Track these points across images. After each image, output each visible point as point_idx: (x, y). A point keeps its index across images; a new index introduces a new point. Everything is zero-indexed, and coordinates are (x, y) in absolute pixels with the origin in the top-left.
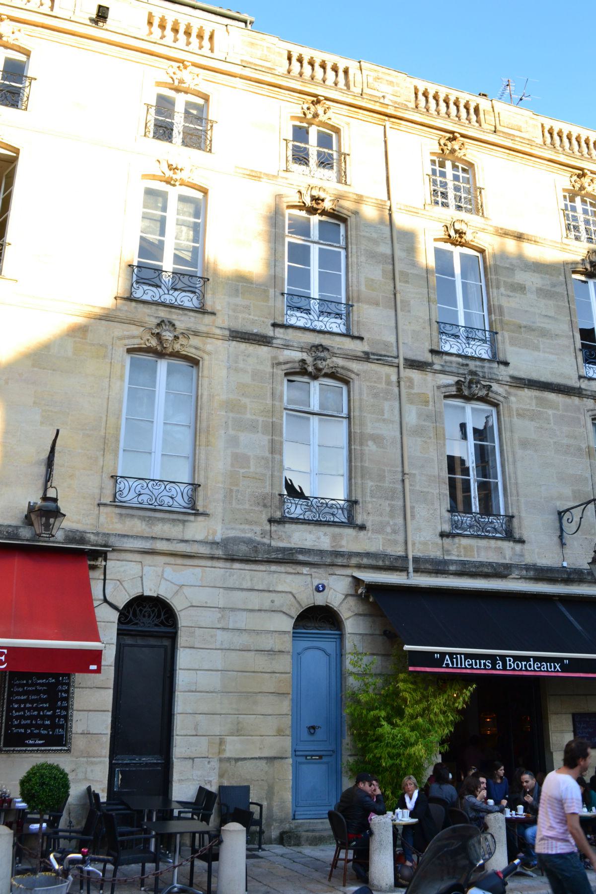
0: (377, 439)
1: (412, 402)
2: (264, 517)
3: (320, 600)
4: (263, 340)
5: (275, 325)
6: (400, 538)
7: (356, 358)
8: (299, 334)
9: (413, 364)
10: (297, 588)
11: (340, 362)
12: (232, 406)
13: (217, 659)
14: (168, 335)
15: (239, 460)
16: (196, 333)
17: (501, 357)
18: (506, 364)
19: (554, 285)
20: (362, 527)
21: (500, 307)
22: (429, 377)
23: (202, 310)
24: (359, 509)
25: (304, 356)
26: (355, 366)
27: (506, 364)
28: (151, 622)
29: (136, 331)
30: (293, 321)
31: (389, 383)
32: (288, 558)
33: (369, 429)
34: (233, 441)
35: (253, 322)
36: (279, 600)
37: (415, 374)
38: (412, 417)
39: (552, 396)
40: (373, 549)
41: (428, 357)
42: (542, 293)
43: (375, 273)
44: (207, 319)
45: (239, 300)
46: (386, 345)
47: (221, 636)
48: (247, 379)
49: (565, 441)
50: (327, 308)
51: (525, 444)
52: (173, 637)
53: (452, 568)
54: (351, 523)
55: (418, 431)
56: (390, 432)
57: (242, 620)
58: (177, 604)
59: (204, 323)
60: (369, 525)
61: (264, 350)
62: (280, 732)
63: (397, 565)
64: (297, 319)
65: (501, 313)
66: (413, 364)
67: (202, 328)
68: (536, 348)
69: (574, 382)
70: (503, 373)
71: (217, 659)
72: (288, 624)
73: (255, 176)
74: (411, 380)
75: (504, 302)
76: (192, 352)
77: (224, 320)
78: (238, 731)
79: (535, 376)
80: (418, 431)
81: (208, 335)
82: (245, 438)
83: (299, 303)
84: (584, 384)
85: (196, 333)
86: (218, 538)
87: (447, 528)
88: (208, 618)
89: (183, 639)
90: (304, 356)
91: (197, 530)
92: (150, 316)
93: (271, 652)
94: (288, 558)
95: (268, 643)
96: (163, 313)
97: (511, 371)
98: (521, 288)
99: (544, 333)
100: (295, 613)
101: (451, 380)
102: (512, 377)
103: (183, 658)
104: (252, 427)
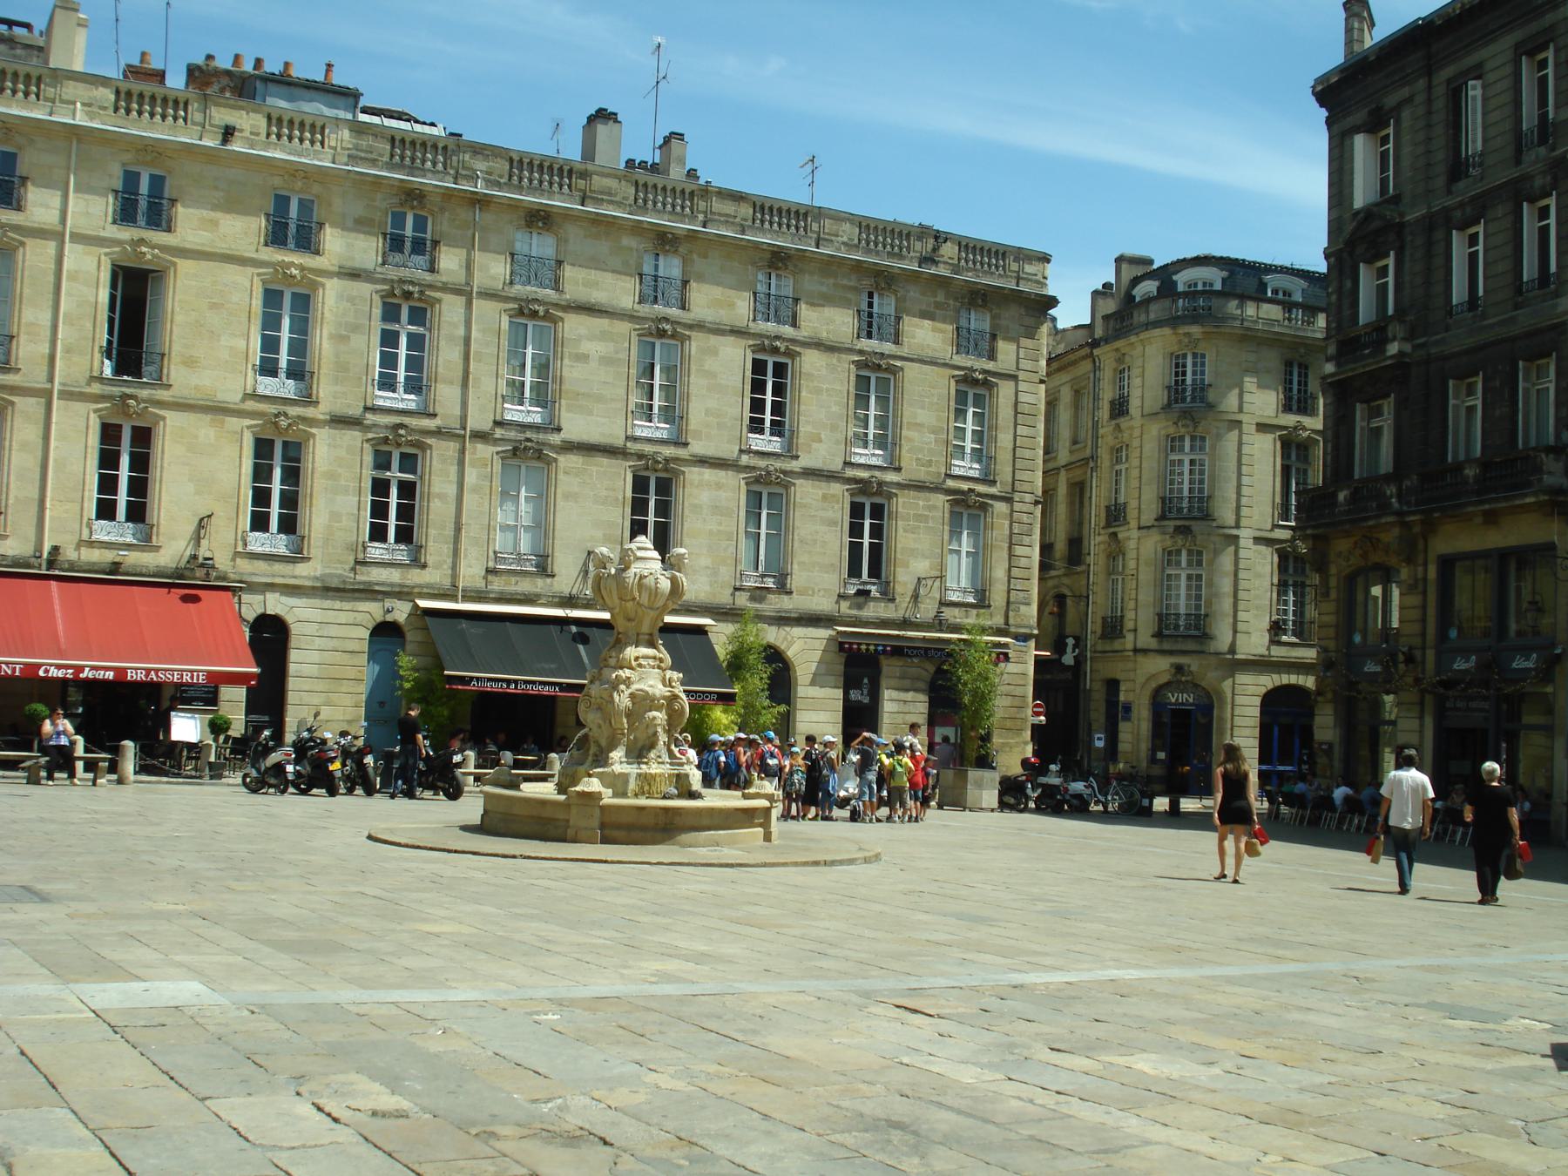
3: (389, 618)
5: (366, 409)
10: (373, 611)
12: (331, 476)
13: (316, 656)
15: (335, 516)
30: (380, 403)
35: (349, 406)
36: (360, 617)
42: (606, 361)
45: (338, 388)
47: (318, 642)
48: (342, 453)
49: (605, 493)
51: (567, 497)
55: (475, 490)
58: (289, 619)
59: (309, 412)
60: (430, 563)
68: (590, 413)
69: (619, 441)
70: (555, 439)
71: (316, 656)
72: (366, 634)
73: (354, 275)
80: (475, 490)
86: (318, 574)
88: (311, 629)
89: (293, 642)
91: (302, 569)
97: (563, 435)
98: (583, 358)
99: (600, 399)
100: (371, 625)
103: (294, 655)
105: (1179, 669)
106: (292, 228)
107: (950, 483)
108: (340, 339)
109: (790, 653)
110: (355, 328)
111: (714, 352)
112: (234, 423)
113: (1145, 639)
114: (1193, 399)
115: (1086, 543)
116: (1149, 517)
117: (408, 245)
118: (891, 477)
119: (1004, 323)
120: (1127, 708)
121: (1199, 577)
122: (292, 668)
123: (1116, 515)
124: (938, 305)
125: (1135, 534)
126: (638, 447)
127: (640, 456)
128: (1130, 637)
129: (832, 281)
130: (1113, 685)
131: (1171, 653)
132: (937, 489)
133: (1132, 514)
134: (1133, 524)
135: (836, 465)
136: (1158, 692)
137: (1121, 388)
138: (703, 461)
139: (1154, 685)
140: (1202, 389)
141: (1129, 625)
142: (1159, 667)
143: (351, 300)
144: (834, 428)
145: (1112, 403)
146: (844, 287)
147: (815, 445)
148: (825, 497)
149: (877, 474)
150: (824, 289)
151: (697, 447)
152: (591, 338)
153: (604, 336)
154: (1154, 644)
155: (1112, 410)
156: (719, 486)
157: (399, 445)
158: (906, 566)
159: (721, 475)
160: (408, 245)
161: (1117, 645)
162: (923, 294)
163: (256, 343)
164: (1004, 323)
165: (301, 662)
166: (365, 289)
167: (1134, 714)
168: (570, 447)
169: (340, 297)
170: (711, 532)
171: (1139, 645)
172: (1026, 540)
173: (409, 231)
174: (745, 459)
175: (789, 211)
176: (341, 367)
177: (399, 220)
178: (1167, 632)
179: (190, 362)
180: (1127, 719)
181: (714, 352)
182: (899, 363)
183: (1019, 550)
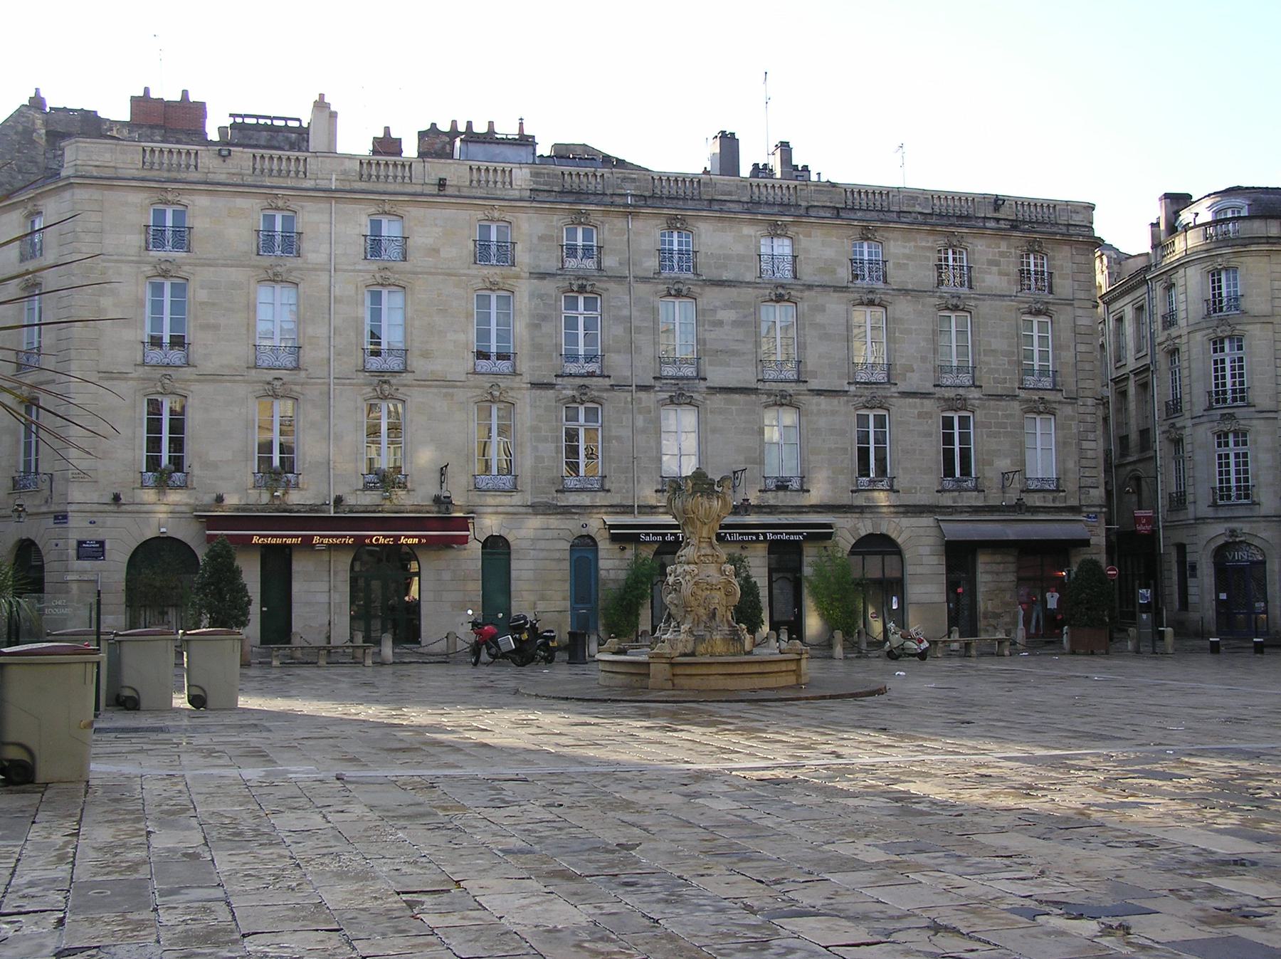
0: (618, 438)
1: (640, 413)
2: (553, 490)
4: (550, 386)
6: (631, 495)
7: (607, 390)
8: (571, 379)
9: (642, 388)
10: (572, 526)
11: (596, 394)
12: (534, 429)
13: (531, 565)
14: (496, 393)
15: (538, 459)
16: (512, 389)
17: (702, 375)
18: (705, 379)
19: (745, 317)
20: (609, 491)
21: (704, 340)
22: (652, 395)
23: (515, 373)
24: (606, 480)
25: (575, 393)
26: (605, 395)
27: (705, 379)
28: (496, 548)
29: (479, 392)
31: (626, 402)
32: (566, 511)
33: (613, 433)
34: (535, 449)
37: (643, 395)
38: (640, 422)
39: (737, 396)
40: (614, 503)
41: (652, 382)
42: (735, 324)
43: (618, 330)
44: (518, 378)
45: (536, 364)
46: (626, 378)
50: (590, 358)
51: (714, 431)
52: (509, 554)
53: (661, 510)
54: (603, 489)
56: (626, 433)
57: (542, 544)
58: (510, 538)
61: (551, 393)
62: (564, 599)
63: (627, 509)
64: (572, 368)
65: (705, 344)
66: (642, 388)
67: (516, 385)
68: (728, 365)
71: (531, 565)
73: (542, 276)
74: (640, 399)
75: (708, 336)
76: (510, 400)
77: (527, 378)
78: (543, 598)
79: (725, 385)
81: (520, 389)
82: (541, 446)
83: (573, 357)
84: (760, 386)
85: (512, 389)
87: (659, 487)
88: (525, 544)
89: (513, 556)
90: (575, 393)
92: (486, 382)
93: (559, 560)
94: (566, 511)
95: (557, 555)
96: (492, 379)
97: (709, 384)
98: (720, 323)
99: (734, 353)
101: (666, 395)
102: (708, 388)
103: (514, 565)
104: (546, 440)
105: (1233, 532)
106: (494, 249)
107: (1023, 394)
108: (535, 326)
109: (899, 541)
110: (544, 318)
111: (822, 309)
112: (460, 394)
113: (1203, 509)
114: (1229, 308)
115: (1152, 432)
116: (1199, 409)
117: (580, 252)
118: (974, 393)
119: (1058, 263)
120: (1193, 568)
121: (1245, 455)
122: (514, 574)
123: (1174, 407)
124: (1002, 254)
125: (1189, 423)
126: (767, 386)
127: (769, 393)
128: (1191, 508)
129: (912, 244)
130: (1181, 548)
131: (1227, 519)
132: (1014, 397)
133: (1186, 406)
134: (1187, 415)
135: (928, 387)
136: (1220, 554)
137: (1171, 303)
138: (819, 392)
139: (1213, 546)
140: (1236, 299)
141: (1190, 498)
142: (1216, 532)
143: (541, 297)
144: (924, 359)
145: (1163, 316)
146: (923, 248)
147: (908, 375)
148: (920, 415)
149: (961, 391)
150: (907, 251)
151: (814, 384)
152: (726, 307)
153: (733, 305)
154: (1210, 512)
155: (1164, 322)
156: (834, 413)
157: (582, 402)
158: (991, 463)
159: (835, 402)
160: (580, 252)
161: (1181, 516)
162: (989, 247)
163: (473, 336)
164: (1058, 263)
165: (521, 570)
166: (549, 286)
167: (1198, 573)
168: (714, 390)
169: (532, 295)
170: (830, 450)
171: (1200, 515)
172: (1091, 436)
173: (580, 242)
174: (853, 388)
175: (874, 193)
176: (537, 348)
177: (572, 234)
178: (1220, 502)
179: (426, 355)
180: (1194, 576)
181: (822, 309)
182: (973, 303)
183: (1086, 445)
